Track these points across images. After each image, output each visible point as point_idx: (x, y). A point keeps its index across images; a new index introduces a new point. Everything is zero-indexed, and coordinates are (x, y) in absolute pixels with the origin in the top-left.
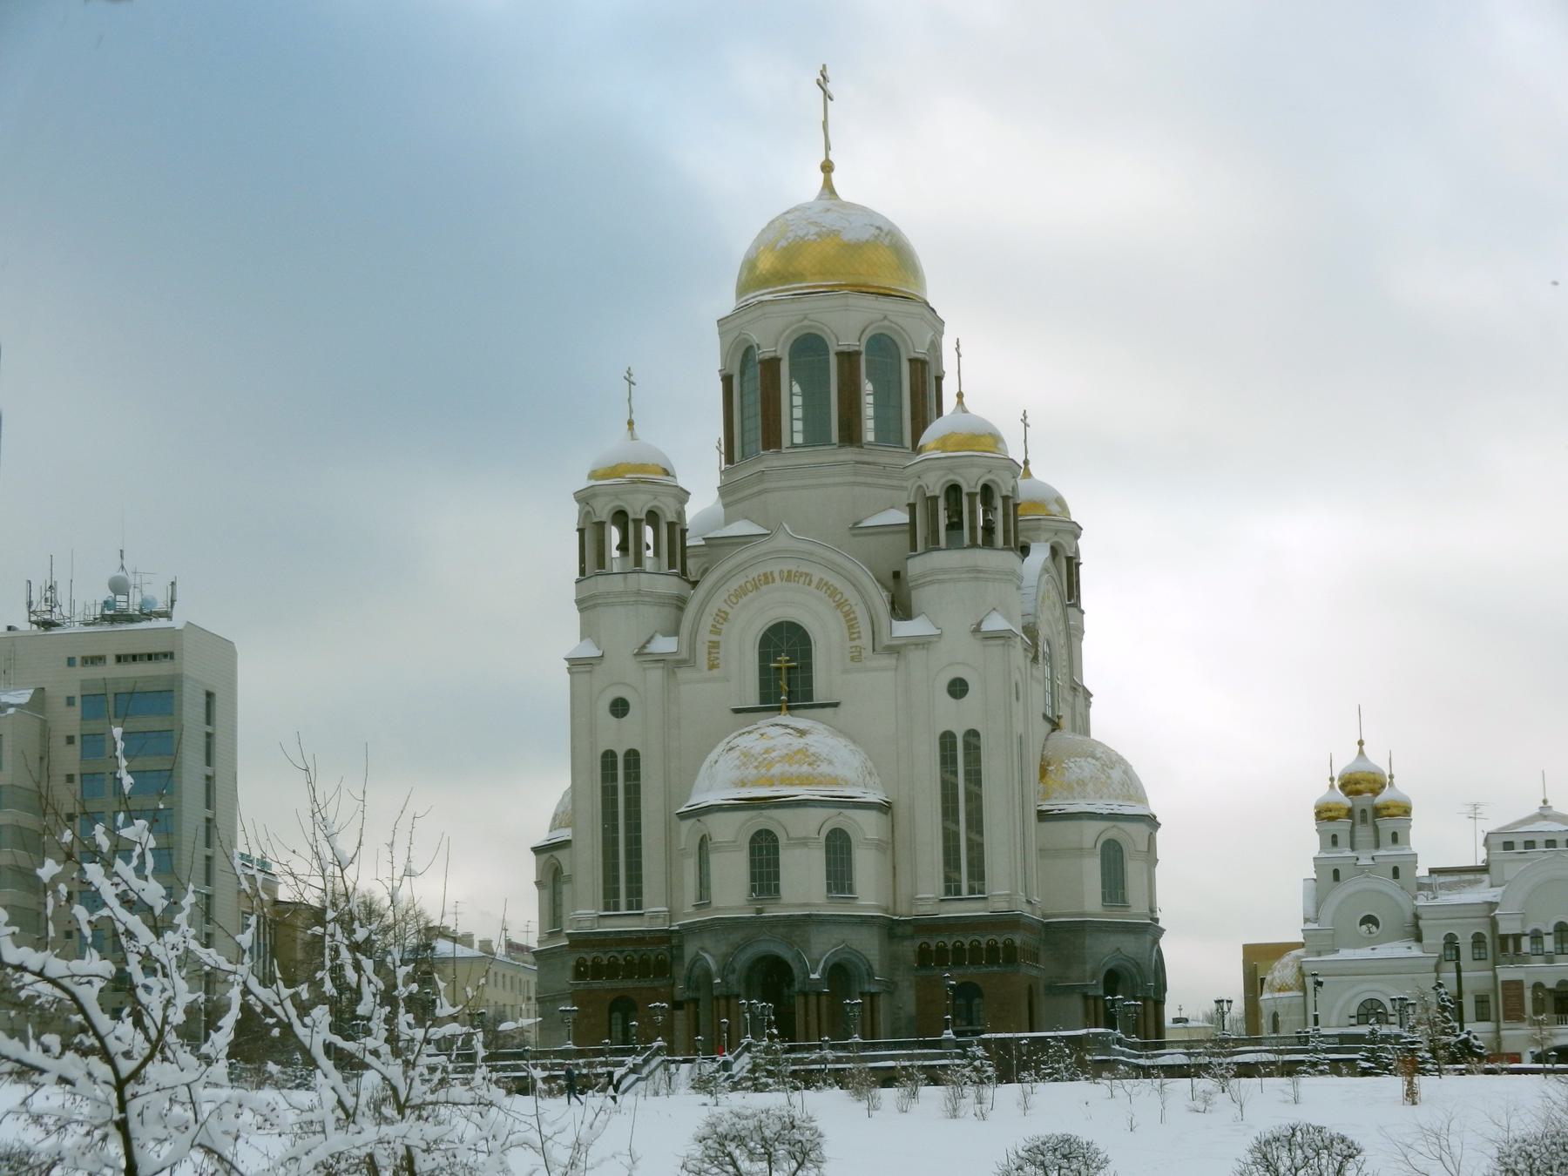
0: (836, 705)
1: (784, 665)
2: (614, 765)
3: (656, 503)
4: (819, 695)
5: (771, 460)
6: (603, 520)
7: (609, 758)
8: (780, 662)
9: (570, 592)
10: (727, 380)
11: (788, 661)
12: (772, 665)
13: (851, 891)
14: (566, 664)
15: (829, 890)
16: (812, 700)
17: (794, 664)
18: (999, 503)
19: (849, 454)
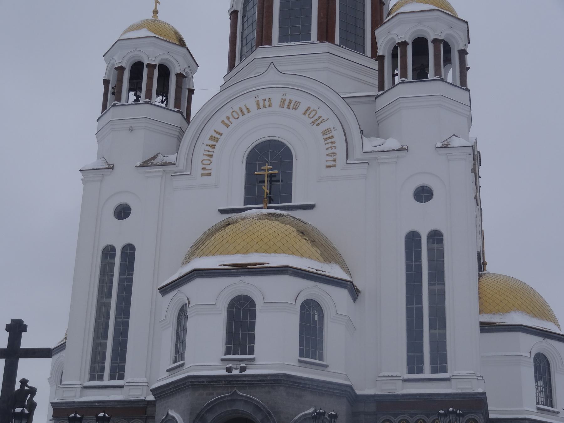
0: (311, 207)
1: (266, 173)
2: (113, 256)
3: (168, 57)
4: (295, 202)
5: (262, 52)
6: (123, 65)
7: (109, 252)
8: (264, 170)
9: (95, 126)
10: (234, 14)
11: (269, 170)
12: (256, 173)
13: (321, 359)
14: (80, 176)
15: (301, 355)
16: (291, 202)
17: (276, 171)
18: (455, 57)
19: (325, 47)
